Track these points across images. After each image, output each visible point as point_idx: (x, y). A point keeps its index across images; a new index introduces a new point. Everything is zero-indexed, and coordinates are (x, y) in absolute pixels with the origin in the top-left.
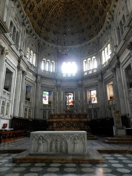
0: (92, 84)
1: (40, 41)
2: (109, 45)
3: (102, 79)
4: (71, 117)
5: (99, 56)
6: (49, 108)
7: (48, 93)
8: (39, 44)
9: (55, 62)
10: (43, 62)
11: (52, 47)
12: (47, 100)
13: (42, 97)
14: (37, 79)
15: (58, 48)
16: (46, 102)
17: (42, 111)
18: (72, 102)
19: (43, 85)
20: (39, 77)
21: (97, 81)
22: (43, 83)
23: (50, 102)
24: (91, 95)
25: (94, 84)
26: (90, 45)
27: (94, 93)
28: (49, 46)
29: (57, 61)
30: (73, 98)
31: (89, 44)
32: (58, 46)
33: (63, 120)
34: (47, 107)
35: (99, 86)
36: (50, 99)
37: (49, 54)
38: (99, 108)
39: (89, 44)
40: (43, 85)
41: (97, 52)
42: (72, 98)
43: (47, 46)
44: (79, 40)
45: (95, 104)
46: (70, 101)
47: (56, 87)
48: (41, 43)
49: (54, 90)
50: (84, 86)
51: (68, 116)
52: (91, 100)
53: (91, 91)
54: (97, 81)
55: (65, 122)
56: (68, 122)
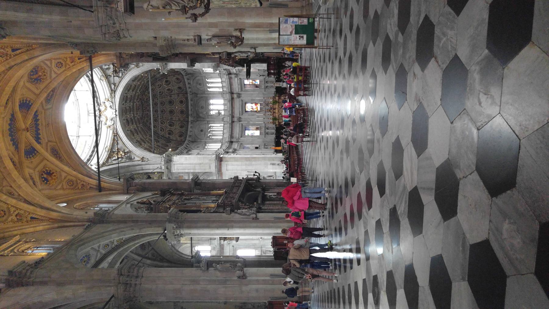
0: (239, 83)
1: (189, 140)
2: (203, 69)
3: (235, 74)
4: (275, 109)
5: (209, 75)
6: (263, 129)
7: (246, 131)
8: (193, 142)
9: (210, 124)
10: (211, 137)
11: (191, 127)
12: (255, 131)
13: (252, 136)
14: (235, 142)
15: (192, 121)
16: (257, 133)
17: (267, 135)
18: (256, 104)
19: (240, 135)
21: (236, 79)
22: (238, 136)
23: (257, 129)
24: (250, 84)
25: (239, 81)
28: (191, 131)
29: (208, 121)
30: (252, 103)
31: (189, 84)
32: (189, 121)
33: (277, 115)
36: (253, 129)
37: (202, 131)
39: (189, 84)
40: (240, 135)
41: (202, 76)
42: (252, 105)
43: (192, 133)
44: (179, 95)
45: (260, 82)
46: (254, 107)
47: (240, 123)
48: (190, 139)
49: (243, 125)
50: (239, 91)
51: (274, 111)
52: (255, 84)
53: (245, 84)
54: (236, 79)
55: (279, 113)
56: (278, 111)
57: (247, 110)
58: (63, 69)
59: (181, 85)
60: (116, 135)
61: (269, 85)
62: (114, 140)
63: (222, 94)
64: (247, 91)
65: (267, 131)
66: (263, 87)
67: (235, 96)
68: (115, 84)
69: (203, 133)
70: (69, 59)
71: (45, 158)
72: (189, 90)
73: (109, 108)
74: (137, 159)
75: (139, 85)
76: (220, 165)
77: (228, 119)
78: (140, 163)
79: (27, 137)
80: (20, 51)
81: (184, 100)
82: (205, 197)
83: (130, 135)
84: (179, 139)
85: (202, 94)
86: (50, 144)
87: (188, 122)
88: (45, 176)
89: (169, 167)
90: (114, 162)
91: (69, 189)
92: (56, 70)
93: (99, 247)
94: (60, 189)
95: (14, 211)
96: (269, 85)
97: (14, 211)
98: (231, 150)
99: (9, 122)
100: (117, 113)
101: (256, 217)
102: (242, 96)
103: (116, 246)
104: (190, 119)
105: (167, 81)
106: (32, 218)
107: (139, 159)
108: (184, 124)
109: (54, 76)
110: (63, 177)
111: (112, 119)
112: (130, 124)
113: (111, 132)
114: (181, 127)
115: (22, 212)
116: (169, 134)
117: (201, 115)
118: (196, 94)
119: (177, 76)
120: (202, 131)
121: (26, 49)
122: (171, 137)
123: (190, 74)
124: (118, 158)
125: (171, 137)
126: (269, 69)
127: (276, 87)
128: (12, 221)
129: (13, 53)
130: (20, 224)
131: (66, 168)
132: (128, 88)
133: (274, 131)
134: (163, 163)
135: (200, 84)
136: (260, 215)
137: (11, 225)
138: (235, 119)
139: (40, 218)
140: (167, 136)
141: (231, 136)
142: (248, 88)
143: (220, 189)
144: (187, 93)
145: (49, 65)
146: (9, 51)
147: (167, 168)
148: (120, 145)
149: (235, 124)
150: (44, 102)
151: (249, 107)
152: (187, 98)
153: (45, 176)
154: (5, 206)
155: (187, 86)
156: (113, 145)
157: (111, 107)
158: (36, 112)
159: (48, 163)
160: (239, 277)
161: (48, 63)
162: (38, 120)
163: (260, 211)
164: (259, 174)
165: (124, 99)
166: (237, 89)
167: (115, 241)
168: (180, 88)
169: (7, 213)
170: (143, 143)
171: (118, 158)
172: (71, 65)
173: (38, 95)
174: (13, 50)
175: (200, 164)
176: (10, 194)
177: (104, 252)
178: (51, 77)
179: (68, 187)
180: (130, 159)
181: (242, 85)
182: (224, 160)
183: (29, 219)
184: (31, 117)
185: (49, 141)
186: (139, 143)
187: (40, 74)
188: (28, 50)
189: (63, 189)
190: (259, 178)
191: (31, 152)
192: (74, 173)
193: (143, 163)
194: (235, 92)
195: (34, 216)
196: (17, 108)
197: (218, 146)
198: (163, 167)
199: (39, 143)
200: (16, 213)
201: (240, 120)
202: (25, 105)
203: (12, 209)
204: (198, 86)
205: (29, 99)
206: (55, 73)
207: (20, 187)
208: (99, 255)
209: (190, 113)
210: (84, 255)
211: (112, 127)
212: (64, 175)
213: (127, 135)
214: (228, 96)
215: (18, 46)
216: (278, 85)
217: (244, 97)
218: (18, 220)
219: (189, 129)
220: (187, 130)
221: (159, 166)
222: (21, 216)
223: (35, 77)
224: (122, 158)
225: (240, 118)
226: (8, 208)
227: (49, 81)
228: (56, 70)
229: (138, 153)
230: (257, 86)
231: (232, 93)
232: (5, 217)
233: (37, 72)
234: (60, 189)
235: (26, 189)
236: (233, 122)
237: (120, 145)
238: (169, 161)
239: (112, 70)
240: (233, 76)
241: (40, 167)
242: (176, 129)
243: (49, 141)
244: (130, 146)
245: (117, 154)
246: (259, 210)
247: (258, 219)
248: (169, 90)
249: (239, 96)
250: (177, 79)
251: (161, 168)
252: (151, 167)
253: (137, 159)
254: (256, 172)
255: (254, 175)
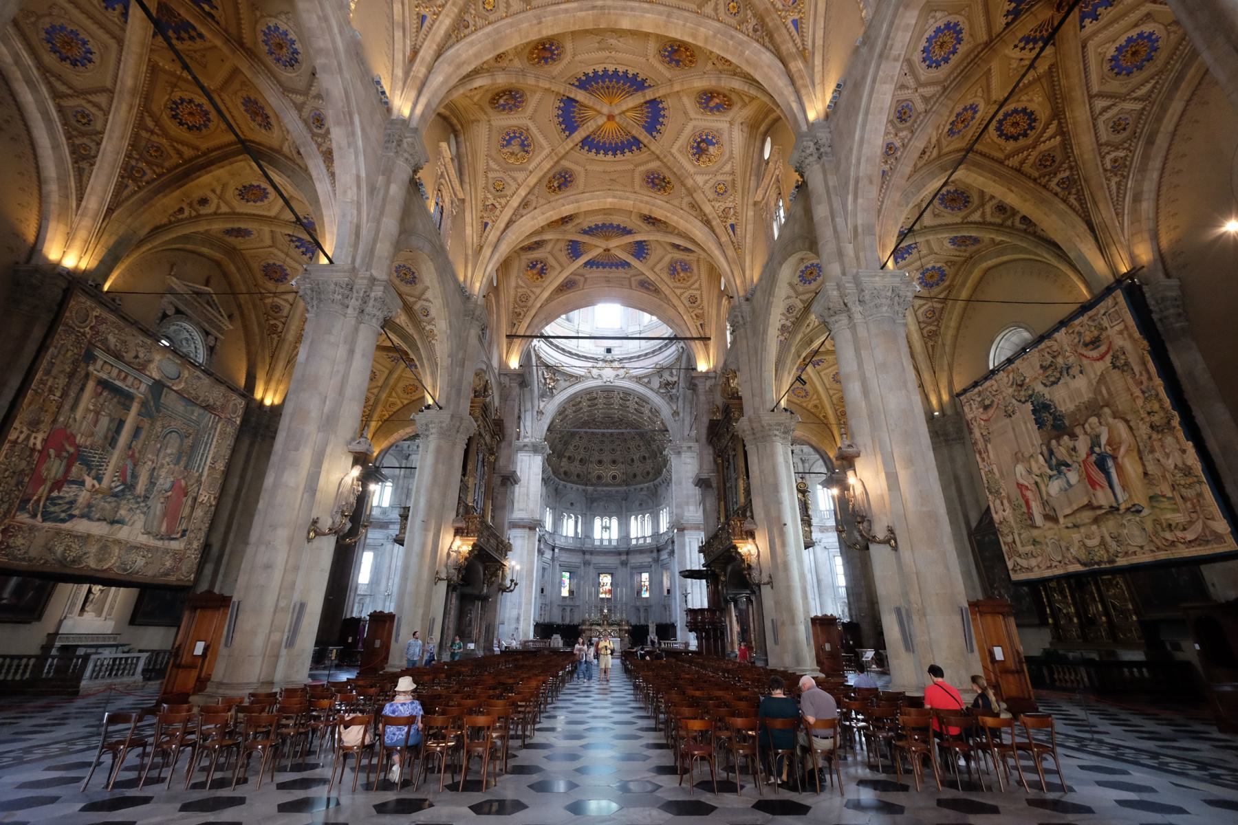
3: (658, 558)
6: (572, 603)
8: (556, 490)
12: (567, 588)
13: (561, 583)
14: (553, 554)
20: (556, 550)
23: (571, 592)
26: (644, 493)
27: (645, 576)
30: (611, 584)
31: (642, 489)
34: (568, 602)
35: (653, 568)
38: (651, 606)
39: (642, 489)
57: (602, 576)
58: (687, 304)
59: (639, 478)
60: (577, 379)
61: (642, 614)
62: (572, 376)
63: (625, 536)
64: (632, 576)
65: (568, 609)
66: (638, 603)
67: (624, 557)
68: (649, 382)
69: (569, 506)
70: (701, 311)
71: (563, 268)
72: (632, 488)
73: (615, 373)
74: (542, 405)
75: (642, 418)
76: (524, 527)
77: (588, 546)
78: (536, 408)
79: (597, 247)
80: (731, 233)
81: (618, 481)
82: (483, 490)
83: (574, 401)
84: (562, 470)
85: (627, 507)
86: (582, 279)
87: (586, 485)
88: (539, 266)
89: (526, 448)
90: (540, 373)
91: (516, 295)
92: (686, 294)
93: (427, 300)
94: (517, 283)
95: (500, 203)
96: (642, 614)
97: (500, 203)
98: (542, 546)
99: (622, 225)
100: (608, 384)
101: (440, 579)
102: (624, 569)
103: (424, 329)
104: (590, 489)
105: (644, 458)
106: (486, 224)
107: (541, 407)
108: (582, 479)
109: (678, 292)
110: (534, 289)
111: (600, 375)
112: (589, 403)
113: (583, 374)
114: (578, 476)
115: (497, 212)
116: (569, 458)
117: (595, 504)
118: (626, 498)
119: (652, 472)
120: (572, 504)
121: (735, 241)
122: (564, 460)
123: (656, 491)
124: (545, 379)
125: (564, 460)
126: (702, 610)
127: (647, 626)
128: (487, 198)
129: (728, 225)
130: (480, 207)
131: (546, 295)
132: (643, 400)
133: (567, 621)
134: (533, 440)
135: (641, 505)
136: (443, 586)
137: (481, 196)
138: (588, 557)
139: (485, 234)
140: (567, 454)
141: (561, 549)
142: (636, 578)
143: (493, 517)
144: (627, 485)
145: (694, 287)
146: (732, 221)
147: (525, 446)
148: (563, 384)
149: (581, 555)
150: (642, 277)
151: (606, 580)
152: (619, 485)
153: (539, 266)
154: (509, 193)
155: (639, 486)
156: (564, 374)
157: (618, 375)
158: (628, 265)
159: (556, 273)
160: (315, 522)
161: (696, 285)
162: (617, 268)
163: (450, 588)
164: (511, 591)
165: (626, 394)
166: (633, 561)
167: (433, 327)
168: (635, 476)
169: (499, 193)
170: (561, 417)
171: (545, 379)
172: (693, 314)
173: (652, 269)
174: (732, 226)
175: (528, 495)
176: (525, 204)
177: (417, 307)
178: (678, 288)
179: (519, 294)
180: (542, 396)
181: (641, 569)
182: (531, 532)
183: (486, 220)
184: (624, 256)
185: (586, 279)
186: (562, 412)
187: (682, 275)
188: (733, 242)
189: (518, 287)
190: (504, 590)
191: (575, 250)
192: (539, 305)
193: (535, 413)
194: (630, 557)
195: (489, 227)
196: (639, 238)
197: (548, 526)
198: (526, 440)
199: (586, 264)
200: (497, 205)
201: (587, 563)
202: (640, 250)
203: (503, 201)
204: (637, 503)
205: (648, 257)
206: (681, 294)
207: (534, 218)
208: (412, 299)
209: (599, 488)
210: (416, 274)
211: (588, 375)
212: (538, 291)
213: (576, 395)
214: (623, 547)
215: (738, 231)
216: (650, 629)
217: (622, 573)
218: (485, 208)
219: (575, 487)
220: (573, 483)
221: (530, 434)
222: (491, 210)
223: (678, 267)
224: (545, 384)
225: (589, 564)
226: (506, 196)
227: (672, 286)
228: (686, 294)
229: (551, 407)
230: (639, 593)
231: (628, 553)
232: (493, 191)
233: (685, 270)
234: (517, 283)
235: (529, 223)
236: (584, 553)
237: (563, 384)
238: (535, 449)
239: (670, 379)
240: (655, 555)
241: (552, 261)
242: (576, 468)
243: (586, 279)
244: (561, 397)
245: (551, 379)
246: (451, 587)
247: (436, 584)
248: (632, 460)
249: (624, 564)
250: (648, 473)
251: (525, 437)
252: (528, 424)
253: (542, 405)
254: (516, 584)
255: (512, 581)
